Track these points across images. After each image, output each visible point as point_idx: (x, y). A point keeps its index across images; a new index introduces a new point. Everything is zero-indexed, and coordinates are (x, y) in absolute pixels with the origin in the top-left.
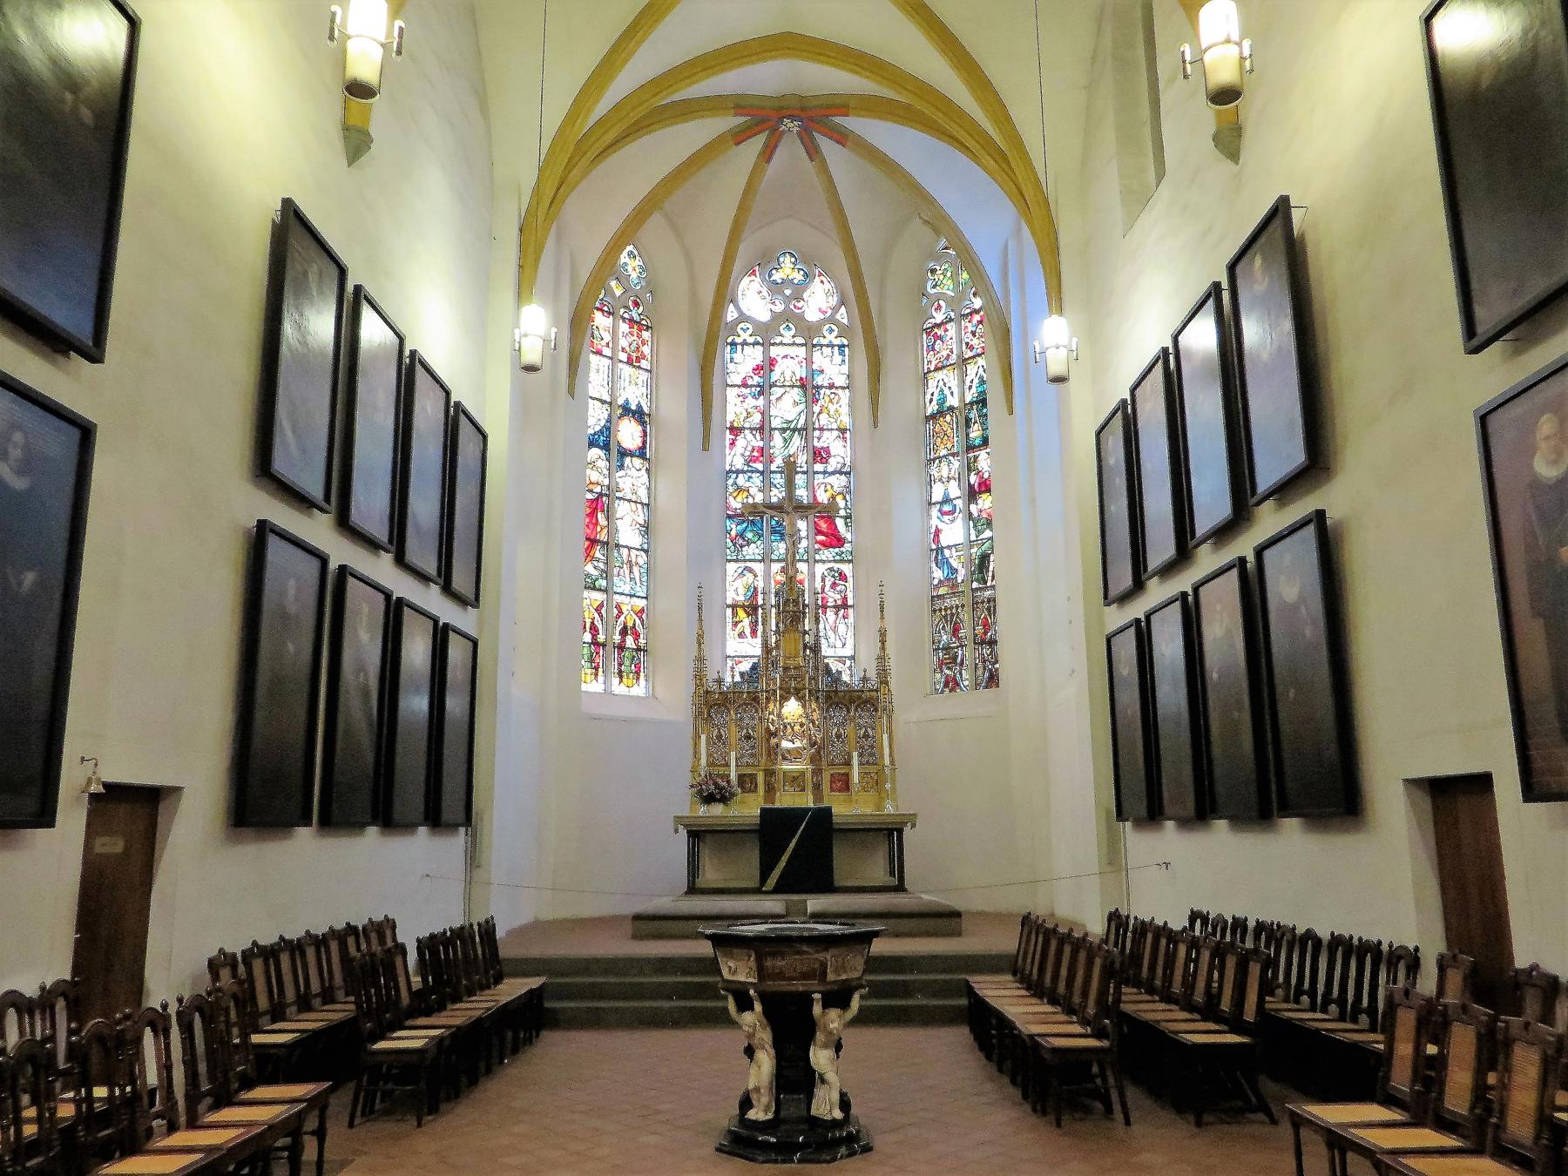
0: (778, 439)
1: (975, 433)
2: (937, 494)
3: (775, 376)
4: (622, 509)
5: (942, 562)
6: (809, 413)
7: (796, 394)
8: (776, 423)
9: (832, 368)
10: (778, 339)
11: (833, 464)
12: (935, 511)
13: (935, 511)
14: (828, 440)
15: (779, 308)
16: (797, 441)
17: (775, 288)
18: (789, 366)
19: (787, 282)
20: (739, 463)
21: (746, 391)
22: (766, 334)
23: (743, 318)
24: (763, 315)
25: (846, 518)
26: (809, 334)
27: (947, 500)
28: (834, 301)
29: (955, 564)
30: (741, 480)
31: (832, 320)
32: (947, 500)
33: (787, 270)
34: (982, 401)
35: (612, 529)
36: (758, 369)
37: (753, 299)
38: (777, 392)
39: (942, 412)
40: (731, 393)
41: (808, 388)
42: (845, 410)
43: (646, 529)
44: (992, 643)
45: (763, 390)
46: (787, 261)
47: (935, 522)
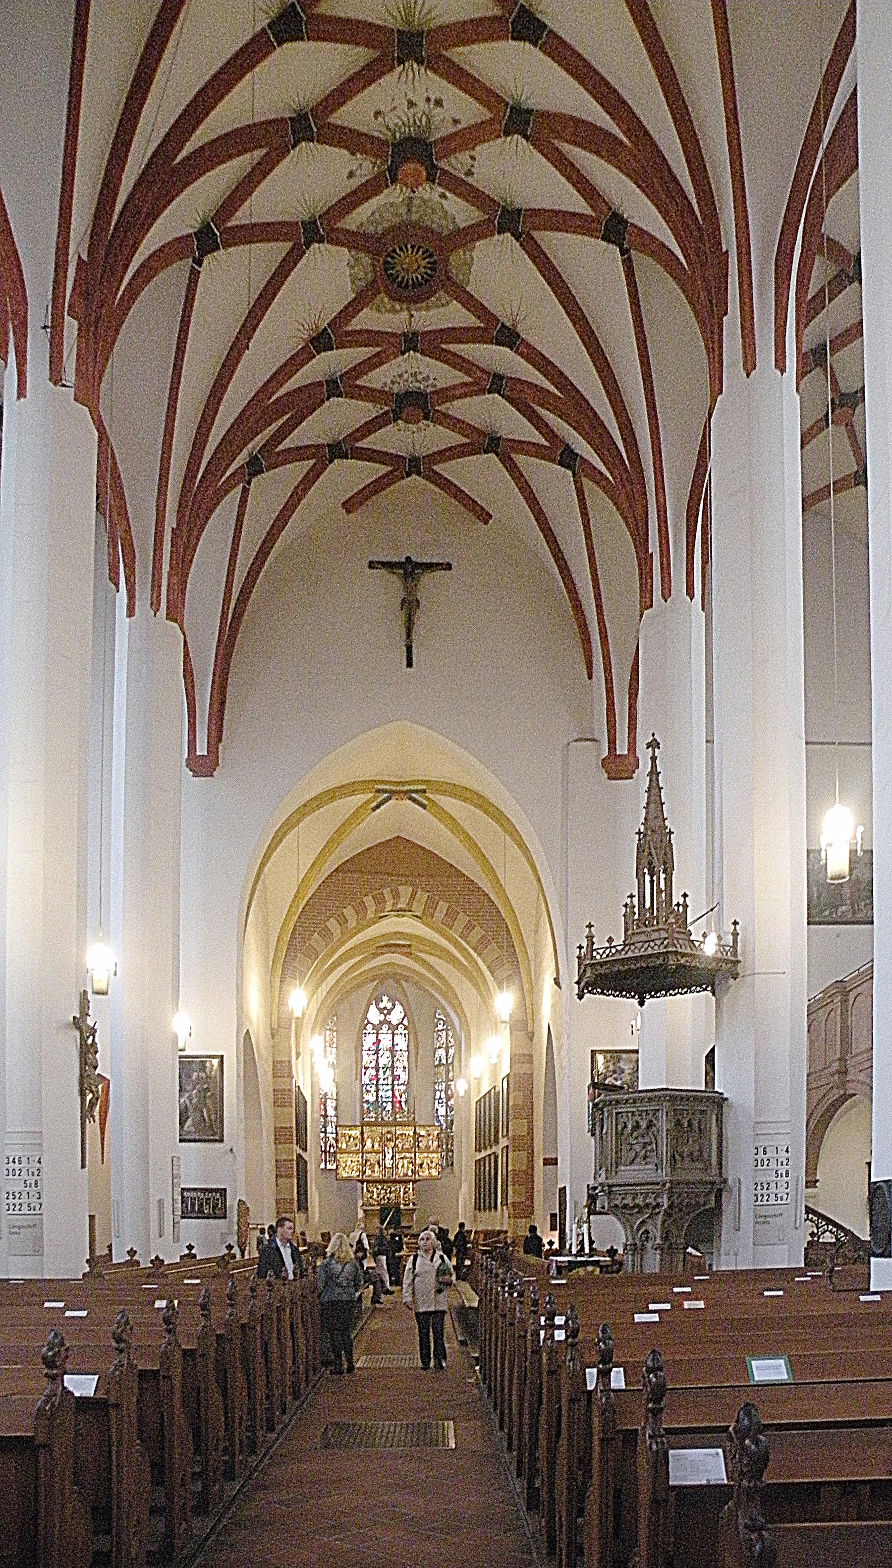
0: (381, 1071)
1: (451, 1075)
2: (437, 1096)
3: (381, 1046)
4: (329, 1101)
5: (439, 1121)
6: (393, 1062)
7: (388, 1054)
8: (381, 1065)
9: (402, 1043)
10: (380, 1032)
11: (401, 1081)
12: (436, 1102)
13: (436, 1102)
14: (400, 1072)
15: (382, 1017)
16: (388, 1072)
17: (381, 1011)
18: (386, 1042)
19: (385, 1008)
20: (367, 1082)
21: (369, 1052)
22: (377, 1028)
23: (369, 1023)
24: (376, 1022)
25: (406, 1102)
26: (393, 1028)
27: (440, 1098)
28: (402, 1015)
29: (442, 1122)
30: (368, 1088)
31: (401, 1023)
32: (440, 1098)
33: (385, 1003)
34: (452, 1063)
35: (326, 1111)
36: (374, 1044)
37: (374, 1016)
38: (381, 1053)
39: (440, 1065)
40: (364, 1053)
41: (392, 1050)
42: (405, 1058)
43: (336, 1109)
44: (452, 1151)
45: (377, 1052)
46: (385, 998)
47: (436, 1106)
